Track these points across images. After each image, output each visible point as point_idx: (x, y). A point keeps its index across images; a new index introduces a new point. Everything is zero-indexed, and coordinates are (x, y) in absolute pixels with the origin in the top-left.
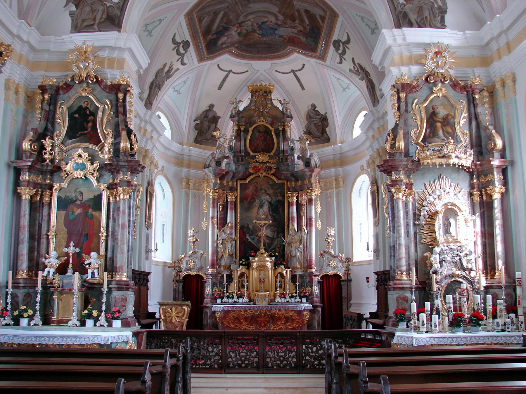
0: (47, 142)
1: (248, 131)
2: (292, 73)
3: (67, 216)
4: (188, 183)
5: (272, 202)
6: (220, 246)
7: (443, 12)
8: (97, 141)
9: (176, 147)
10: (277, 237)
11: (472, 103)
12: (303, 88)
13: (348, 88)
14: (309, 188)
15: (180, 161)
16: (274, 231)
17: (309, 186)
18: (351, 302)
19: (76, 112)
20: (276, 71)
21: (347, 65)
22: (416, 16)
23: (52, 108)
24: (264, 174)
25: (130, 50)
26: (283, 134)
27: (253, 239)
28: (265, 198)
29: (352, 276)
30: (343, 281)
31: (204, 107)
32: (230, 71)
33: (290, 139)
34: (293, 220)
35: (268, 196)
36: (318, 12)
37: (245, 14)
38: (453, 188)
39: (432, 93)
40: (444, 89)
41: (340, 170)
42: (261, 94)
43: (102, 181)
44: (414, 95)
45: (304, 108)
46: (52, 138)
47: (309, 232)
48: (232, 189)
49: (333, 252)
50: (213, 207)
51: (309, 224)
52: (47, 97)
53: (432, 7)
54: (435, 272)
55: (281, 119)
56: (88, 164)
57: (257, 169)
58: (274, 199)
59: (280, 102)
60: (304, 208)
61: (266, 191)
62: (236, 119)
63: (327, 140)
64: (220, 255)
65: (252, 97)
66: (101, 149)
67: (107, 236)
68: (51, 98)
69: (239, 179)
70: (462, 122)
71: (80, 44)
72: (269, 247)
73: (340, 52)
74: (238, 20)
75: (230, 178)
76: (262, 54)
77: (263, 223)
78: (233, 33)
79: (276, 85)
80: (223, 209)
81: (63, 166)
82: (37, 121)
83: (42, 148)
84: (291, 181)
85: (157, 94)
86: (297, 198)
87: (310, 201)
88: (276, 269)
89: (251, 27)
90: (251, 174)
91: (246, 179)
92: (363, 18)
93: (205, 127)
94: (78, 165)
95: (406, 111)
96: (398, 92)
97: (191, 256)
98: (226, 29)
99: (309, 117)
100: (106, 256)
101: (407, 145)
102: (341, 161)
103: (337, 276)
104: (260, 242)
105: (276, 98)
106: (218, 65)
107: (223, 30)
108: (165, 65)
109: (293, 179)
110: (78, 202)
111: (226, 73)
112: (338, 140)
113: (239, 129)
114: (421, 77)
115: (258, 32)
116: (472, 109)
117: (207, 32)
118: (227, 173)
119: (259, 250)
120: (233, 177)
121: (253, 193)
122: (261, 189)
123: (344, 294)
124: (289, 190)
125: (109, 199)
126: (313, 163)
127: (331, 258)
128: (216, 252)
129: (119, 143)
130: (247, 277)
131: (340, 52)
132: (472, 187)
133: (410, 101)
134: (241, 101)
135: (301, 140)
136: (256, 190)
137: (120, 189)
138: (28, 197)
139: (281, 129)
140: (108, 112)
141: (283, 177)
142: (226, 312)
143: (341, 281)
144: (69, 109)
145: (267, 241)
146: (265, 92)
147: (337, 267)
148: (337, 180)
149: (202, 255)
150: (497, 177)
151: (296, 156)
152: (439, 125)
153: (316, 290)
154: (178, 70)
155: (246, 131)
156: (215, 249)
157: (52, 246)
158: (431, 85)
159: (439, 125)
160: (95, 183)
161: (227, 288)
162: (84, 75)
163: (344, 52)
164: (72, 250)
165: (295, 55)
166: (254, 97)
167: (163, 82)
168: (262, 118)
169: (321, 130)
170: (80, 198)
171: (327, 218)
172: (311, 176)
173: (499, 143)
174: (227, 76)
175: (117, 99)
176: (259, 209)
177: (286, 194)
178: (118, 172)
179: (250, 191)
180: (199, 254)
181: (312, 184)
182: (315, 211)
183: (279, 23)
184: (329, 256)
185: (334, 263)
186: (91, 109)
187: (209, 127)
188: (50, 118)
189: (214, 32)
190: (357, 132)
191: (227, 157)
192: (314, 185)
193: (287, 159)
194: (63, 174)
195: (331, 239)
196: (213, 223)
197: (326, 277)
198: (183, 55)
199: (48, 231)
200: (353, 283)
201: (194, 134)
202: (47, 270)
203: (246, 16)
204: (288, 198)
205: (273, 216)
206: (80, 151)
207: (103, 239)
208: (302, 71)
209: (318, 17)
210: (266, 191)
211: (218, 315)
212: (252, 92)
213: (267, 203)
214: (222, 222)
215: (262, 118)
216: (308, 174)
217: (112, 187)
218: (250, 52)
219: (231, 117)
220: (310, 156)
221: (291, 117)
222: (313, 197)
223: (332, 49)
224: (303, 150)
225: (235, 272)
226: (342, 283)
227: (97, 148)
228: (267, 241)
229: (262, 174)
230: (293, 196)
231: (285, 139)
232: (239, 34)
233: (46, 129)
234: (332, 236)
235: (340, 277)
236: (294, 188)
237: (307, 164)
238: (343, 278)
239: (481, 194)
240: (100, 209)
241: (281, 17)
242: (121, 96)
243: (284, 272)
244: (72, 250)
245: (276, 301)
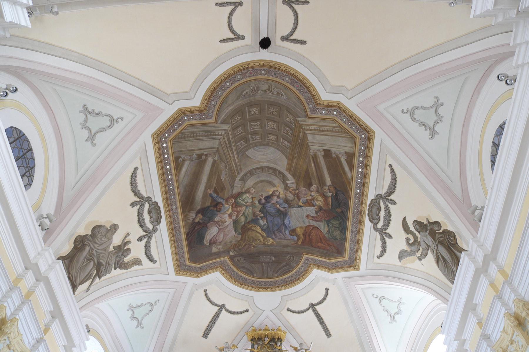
2: (311, 310)
12: (329, 335)
20: (288, 310)
32: (222, 306)
37: (242, 173)
65: (253, 346)
74: (232, 187)
76: (267, 277)
89: (250, 209)
106: (205, 291)
111: (218, 308)
115: (262, 222)
154: (137, 262)
165: (316, 273)
166: (256, 346)
174: (217, 315)
183: (290, 196)
189: (199, 208)
198: (148, 235)
203: (244, 180)
208: (325, 302)
212: (252, 340)
218: (251, 273)
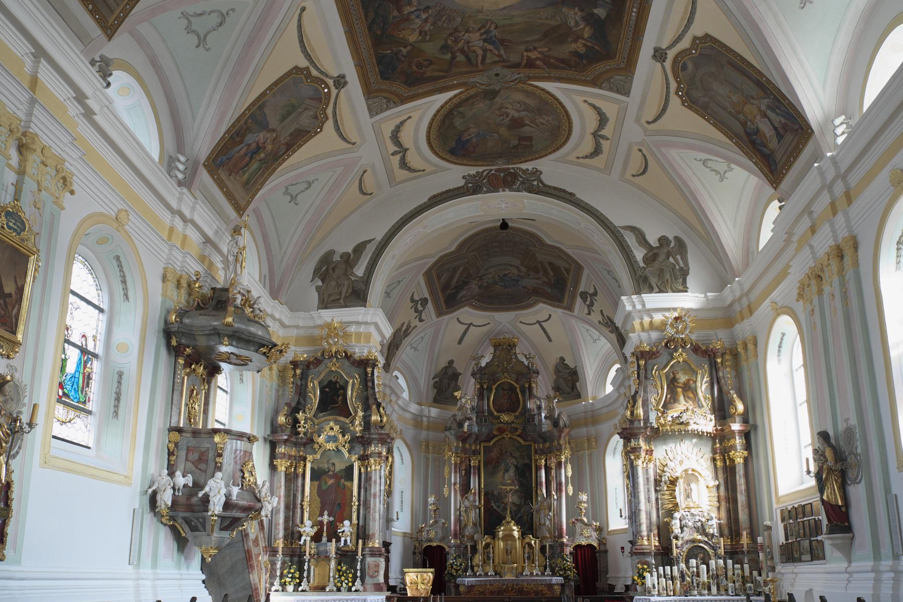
0: (300, 416)
1: (491, 389)
3: (319, 486)
4: (427, 447)
6: (463, 514)
7: (685, 273)
8: (347, 414)
9: (414, 408)
11: (714, 368)
12: (550, 340)
13: (599, 339)
14: (558, 450)
15: (417, 422)
19: (326, 386)
21: (596, 317)
22: (656, 279)
23: (303, 383)
25: (376, 325)
26: (529, 392)
27: (498, 507)
31: (443, 363)
32: (471, 324)
33: (536, 397)
36: (562, 264)
38: (694, 454)
39: (673, 358)
40: (684, 354)
41: (592, 430)
42: (504, 347)
43: (353, 452)
44: (654, 361)
45: (552, 361)
46: (304, 412)
47: (559, 499)
48: (476, 453)
49: (585, 520)
50: (455, 472)
51: (559, 490)
52: (298, 372)
53: (674, 269)
54: (676, 538)
55: (527, 374)
56: (340, 436)
57: (501, 431)
59: (525, 356)
60: (553, 472)
62: (478, 376)
63: (578, 396)
64: (463, 524)
66: (352, 422)
67: (359, 506)
68: (302, 373)
70: (704, 386)
71: (329, 320)
72: (516, 515)
73: (588, 303)
75: (472, 441)
77: (508, 488)
78: (474, 286)
79: (522, 338)
80: (466, 474)
81: (315, 438)
82: (290, 394)
83: (296, 421)
84: (539, 443)
85: (395, 354)
86: (546, 461)
87: (559, 464)
88: (524, 538)
90: (495, 436)
92: (609, 272)
93: (444, 386)
94: (330, 436)
95: (646, 378)
96: (638, 360)
97: (432, 525)
98: (466, 283)
99: (557, 371)
100: (358, 524)
101: (646, 413)
102: (593, 418)
103: (590, 546)
105: (521, 353)
107: (463, 284)
108: (403, 324)
109: (540, 440)
110: (331, 473)
112: (590, 396)
113: (482, 386)
114: (661, 343)
116: (714, 373)
117: (445, 288)
118: (470, 435)
119: (505, 518)
120: (476, 439)
124: (536, 452)
125: (360, 470)
126: (561, 423)
128: (458, 520)
129: (370, 416)
131: (588, 303)
132: (714, 451)
133: (649, 367)
134: (483, 356)
135: (549, 399)
137: (372, 460)
138: (283, 469)
139: (527, 386)
140: (357, 386)
141: (529, 438)
142: (471, 587)
144: (319, 383)
146: (509, 345)
148: (588, 440)
149: (444, 524)
150: (738, 441)
151: (543, 415)
152: (680, 390)
153: (569, 562)
155: (489, 389)
157: (306, 515)
158: (671, 351)
159: (680, 390)
160: (347, 455)
161: (471, 560)
162: (334, 349)
163: (592, 304)
164: (326, 518)
165: (541, 305)
167: (401, 341)
168: (506, 375)
169: (570, 385)
170: (332, 469)
171: (578, 482)
172: (560, 437)
173: (740, 407)
174: (467, 330)
175: (366, 373)
176: (504, 474)
178: (369, 444)
179: (494, 454)
180: (440, 524)
181: (561, 446)
182: (566, 475)
185: (588, 532)
186: (341, 383)
187: (449, 385)
188: (302, 392)
190: (609, 389)
191: (470, 419)
193: (533, 419)
194: (316, 446)
196: (455, 489)
197: (578, 547)
198: (421, 312)
199: (302, 501)
200: (609, 554)
201: (433, 393)
202: (303, 538)
204: (536, 461)
206: (332, 424)
207: (355, 508)
209: (563, 269)
211: (462, 589)
214: (465, 489)
215: (506, 375)
216: (556, 434)
217: (363, 458)
220: (559, 415)
221: (538, 373)
223: (579, 300)
224: (551, 411)
226: (597, 555)
227: (347, 421)
230: (541, 459)
231: (531, 396)
232: (480, 287)
233: (298, 403)
236: (541, 450)
237: (556, 423)
239: (724, 459)
240: (352, 479)
241: (523, 269)
242: (369, 370)
243: (533, 542)
244: (326, 518)
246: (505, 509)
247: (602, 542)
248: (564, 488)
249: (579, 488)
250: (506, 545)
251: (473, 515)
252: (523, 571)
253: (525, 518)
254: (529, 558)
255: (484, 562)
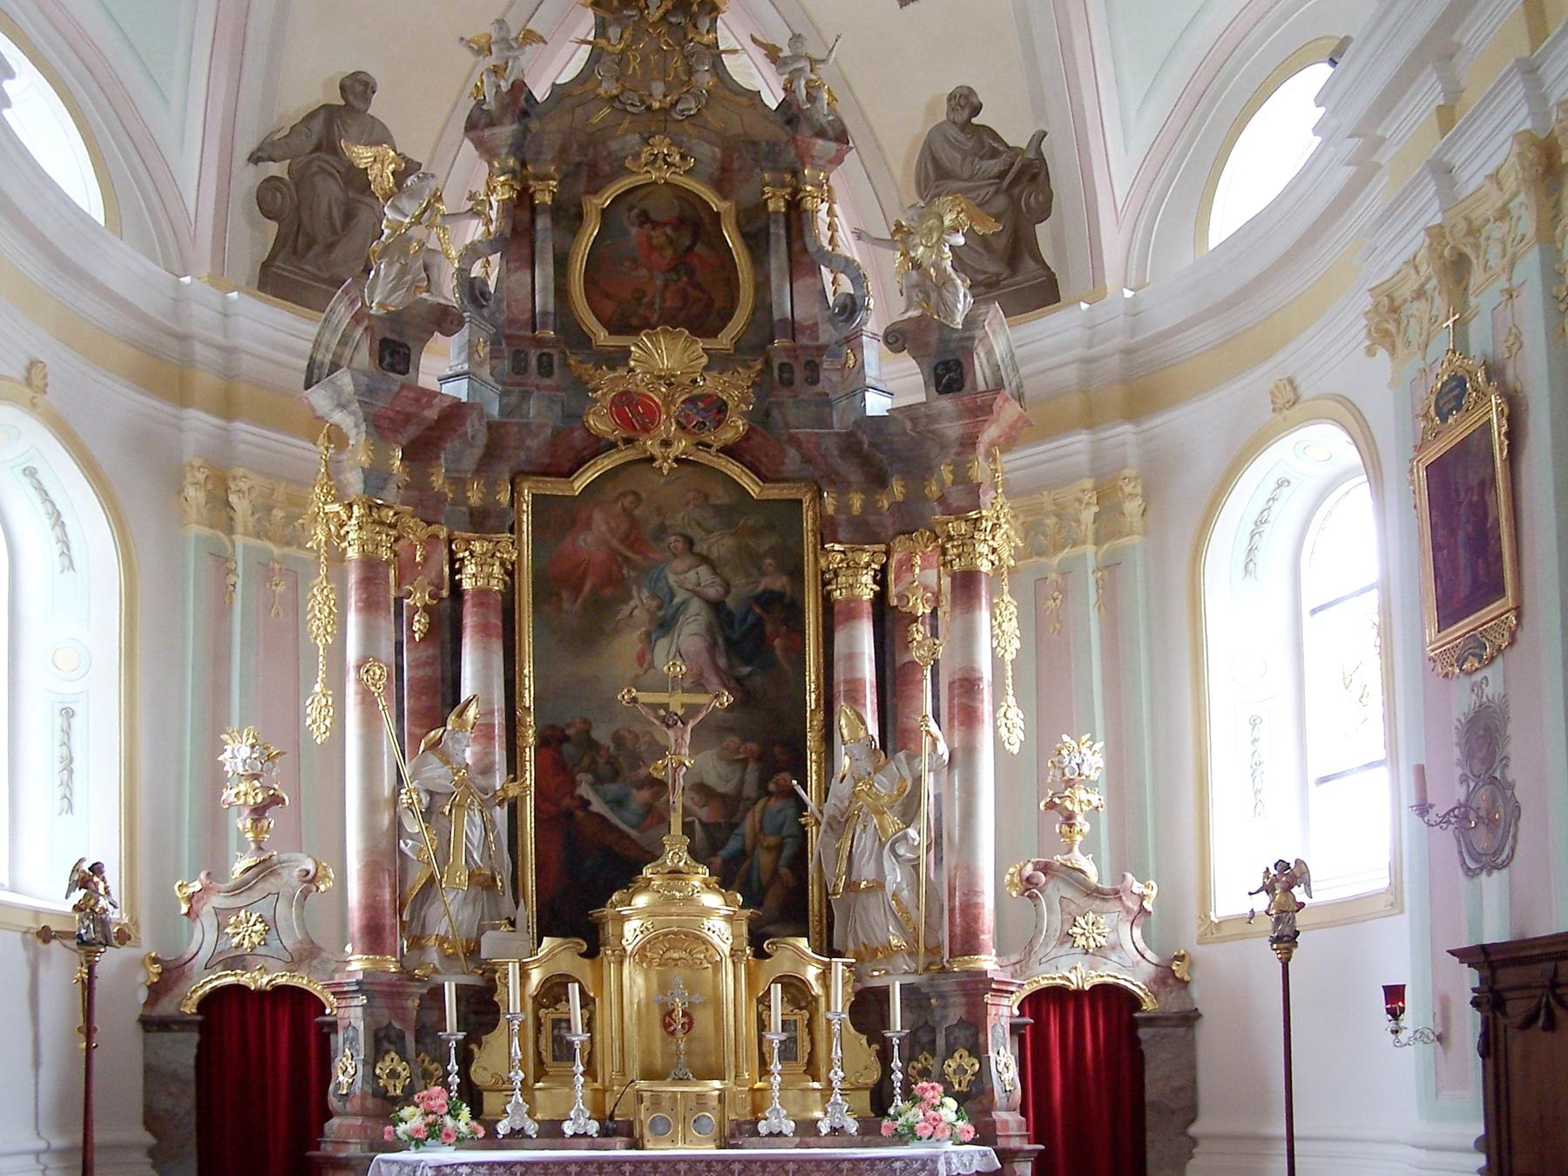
5: (730, 602)
10: (764, 791)
14: (959, 513)
16: (744, 762)
17: (957, 498)
18: (1193, 1130)
24: (681, 446)
28: (689, 579)
29: (1199, 995)
30: (1151, 1021)
34: (854, 697)
35: (703, 570)
58: (742, 587)
61: (690, 543)
62: (506, 132)
69: (527, 474)
72: (714, 848)
87: (966, 585)
90: (601, 446)
91: (569, 474)
103: (1113, 998)
104: (664, 821)
121: (614, 554)
122: (662, 531)
123: (1154, 1089)
127: (1082, 901)
130: (586, 1002)
136: (634, 536)
143: (1134, 1025)
145: (704, 813)
147: (1116, 947)
156: (384, 844)
172: (969, 443)
177: (809, 558)
181: (974, 490)
184: (1068, 893)
192: (986, 498)
195: (1082, 800)
200: (1206, 1032)
205: (738, 680)
210: (690, 543)
213: (696, 606)
216: (952, 429)
219: (471, 126)
222: (985, 566)
225: (513, 970)
226: (1143, 1033)
228: (704, 813)
229: (666, 443)
230: (855, 568)
234: (1090, 785)
235: (1133, 1001)
238: (1149, 1005)
245: (763, 1127)
246: (655, 816)
247: (1168, 977)
248: (986, 707)
249: (1050, 717)
250: (664, 986)
251: (473, 832)
252: (757, 1110)
253: (764, 859)
254: (788, 1052)
255: (540, 1072)
